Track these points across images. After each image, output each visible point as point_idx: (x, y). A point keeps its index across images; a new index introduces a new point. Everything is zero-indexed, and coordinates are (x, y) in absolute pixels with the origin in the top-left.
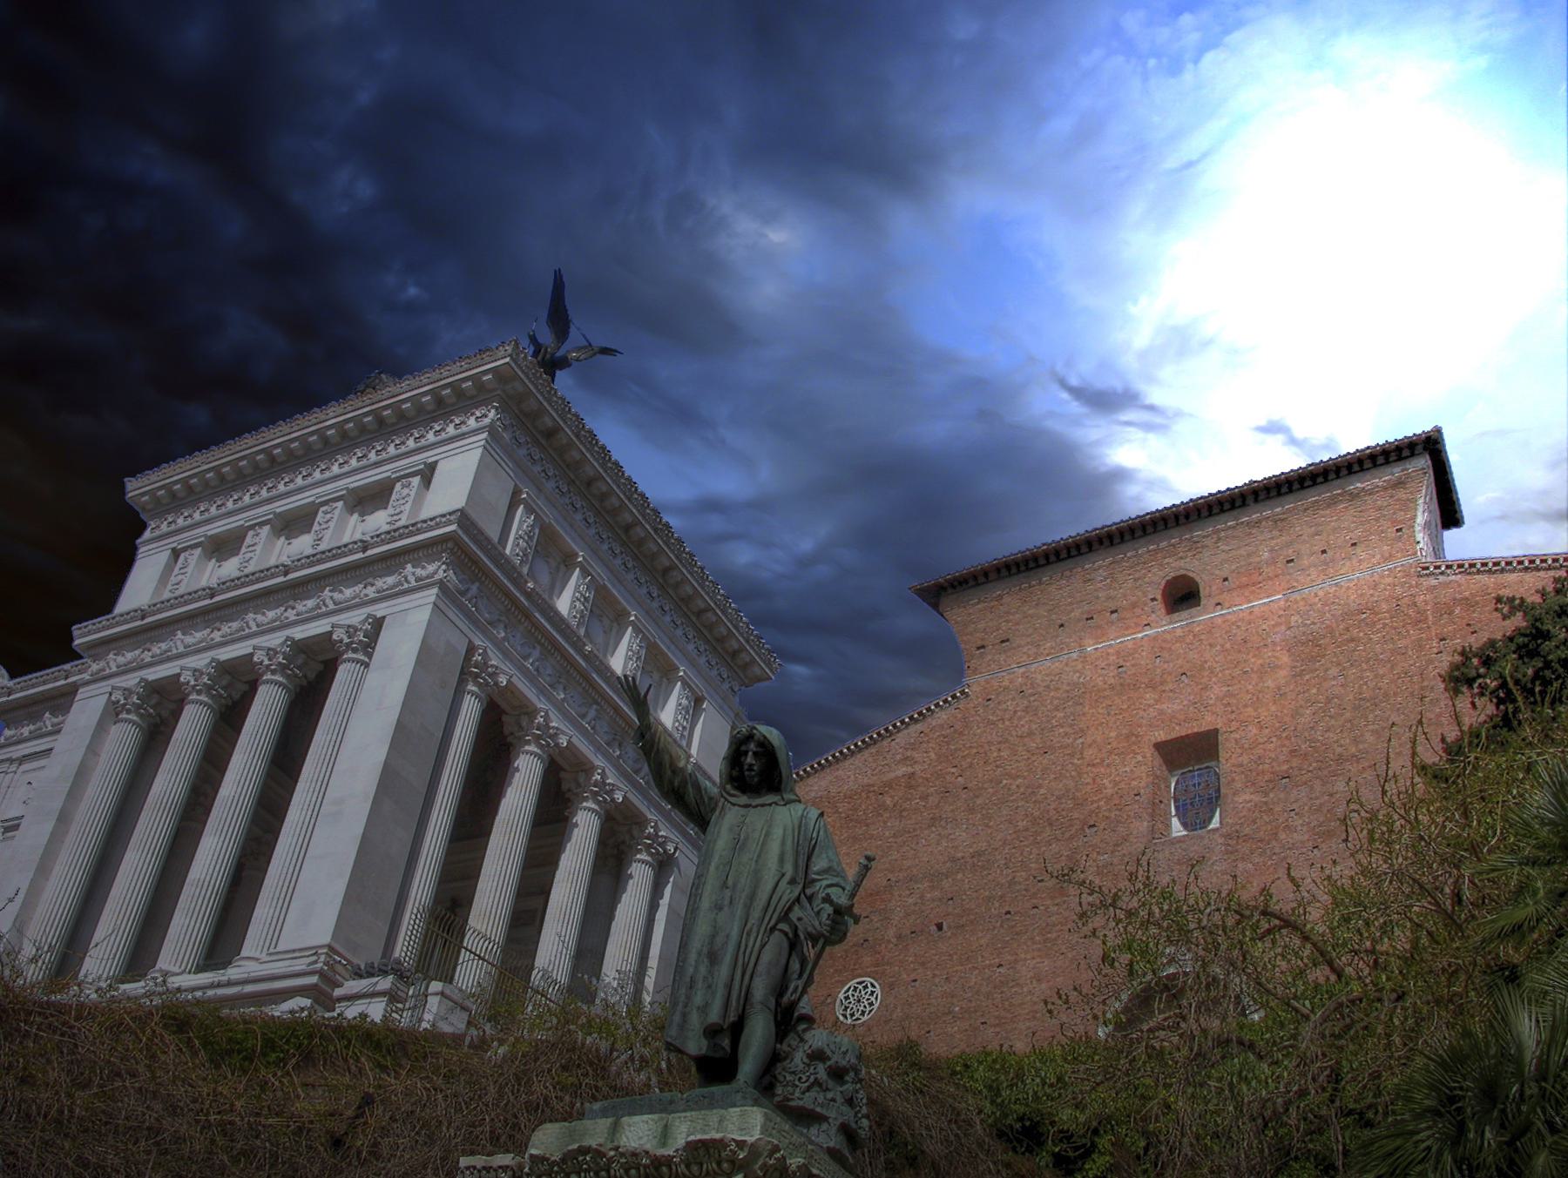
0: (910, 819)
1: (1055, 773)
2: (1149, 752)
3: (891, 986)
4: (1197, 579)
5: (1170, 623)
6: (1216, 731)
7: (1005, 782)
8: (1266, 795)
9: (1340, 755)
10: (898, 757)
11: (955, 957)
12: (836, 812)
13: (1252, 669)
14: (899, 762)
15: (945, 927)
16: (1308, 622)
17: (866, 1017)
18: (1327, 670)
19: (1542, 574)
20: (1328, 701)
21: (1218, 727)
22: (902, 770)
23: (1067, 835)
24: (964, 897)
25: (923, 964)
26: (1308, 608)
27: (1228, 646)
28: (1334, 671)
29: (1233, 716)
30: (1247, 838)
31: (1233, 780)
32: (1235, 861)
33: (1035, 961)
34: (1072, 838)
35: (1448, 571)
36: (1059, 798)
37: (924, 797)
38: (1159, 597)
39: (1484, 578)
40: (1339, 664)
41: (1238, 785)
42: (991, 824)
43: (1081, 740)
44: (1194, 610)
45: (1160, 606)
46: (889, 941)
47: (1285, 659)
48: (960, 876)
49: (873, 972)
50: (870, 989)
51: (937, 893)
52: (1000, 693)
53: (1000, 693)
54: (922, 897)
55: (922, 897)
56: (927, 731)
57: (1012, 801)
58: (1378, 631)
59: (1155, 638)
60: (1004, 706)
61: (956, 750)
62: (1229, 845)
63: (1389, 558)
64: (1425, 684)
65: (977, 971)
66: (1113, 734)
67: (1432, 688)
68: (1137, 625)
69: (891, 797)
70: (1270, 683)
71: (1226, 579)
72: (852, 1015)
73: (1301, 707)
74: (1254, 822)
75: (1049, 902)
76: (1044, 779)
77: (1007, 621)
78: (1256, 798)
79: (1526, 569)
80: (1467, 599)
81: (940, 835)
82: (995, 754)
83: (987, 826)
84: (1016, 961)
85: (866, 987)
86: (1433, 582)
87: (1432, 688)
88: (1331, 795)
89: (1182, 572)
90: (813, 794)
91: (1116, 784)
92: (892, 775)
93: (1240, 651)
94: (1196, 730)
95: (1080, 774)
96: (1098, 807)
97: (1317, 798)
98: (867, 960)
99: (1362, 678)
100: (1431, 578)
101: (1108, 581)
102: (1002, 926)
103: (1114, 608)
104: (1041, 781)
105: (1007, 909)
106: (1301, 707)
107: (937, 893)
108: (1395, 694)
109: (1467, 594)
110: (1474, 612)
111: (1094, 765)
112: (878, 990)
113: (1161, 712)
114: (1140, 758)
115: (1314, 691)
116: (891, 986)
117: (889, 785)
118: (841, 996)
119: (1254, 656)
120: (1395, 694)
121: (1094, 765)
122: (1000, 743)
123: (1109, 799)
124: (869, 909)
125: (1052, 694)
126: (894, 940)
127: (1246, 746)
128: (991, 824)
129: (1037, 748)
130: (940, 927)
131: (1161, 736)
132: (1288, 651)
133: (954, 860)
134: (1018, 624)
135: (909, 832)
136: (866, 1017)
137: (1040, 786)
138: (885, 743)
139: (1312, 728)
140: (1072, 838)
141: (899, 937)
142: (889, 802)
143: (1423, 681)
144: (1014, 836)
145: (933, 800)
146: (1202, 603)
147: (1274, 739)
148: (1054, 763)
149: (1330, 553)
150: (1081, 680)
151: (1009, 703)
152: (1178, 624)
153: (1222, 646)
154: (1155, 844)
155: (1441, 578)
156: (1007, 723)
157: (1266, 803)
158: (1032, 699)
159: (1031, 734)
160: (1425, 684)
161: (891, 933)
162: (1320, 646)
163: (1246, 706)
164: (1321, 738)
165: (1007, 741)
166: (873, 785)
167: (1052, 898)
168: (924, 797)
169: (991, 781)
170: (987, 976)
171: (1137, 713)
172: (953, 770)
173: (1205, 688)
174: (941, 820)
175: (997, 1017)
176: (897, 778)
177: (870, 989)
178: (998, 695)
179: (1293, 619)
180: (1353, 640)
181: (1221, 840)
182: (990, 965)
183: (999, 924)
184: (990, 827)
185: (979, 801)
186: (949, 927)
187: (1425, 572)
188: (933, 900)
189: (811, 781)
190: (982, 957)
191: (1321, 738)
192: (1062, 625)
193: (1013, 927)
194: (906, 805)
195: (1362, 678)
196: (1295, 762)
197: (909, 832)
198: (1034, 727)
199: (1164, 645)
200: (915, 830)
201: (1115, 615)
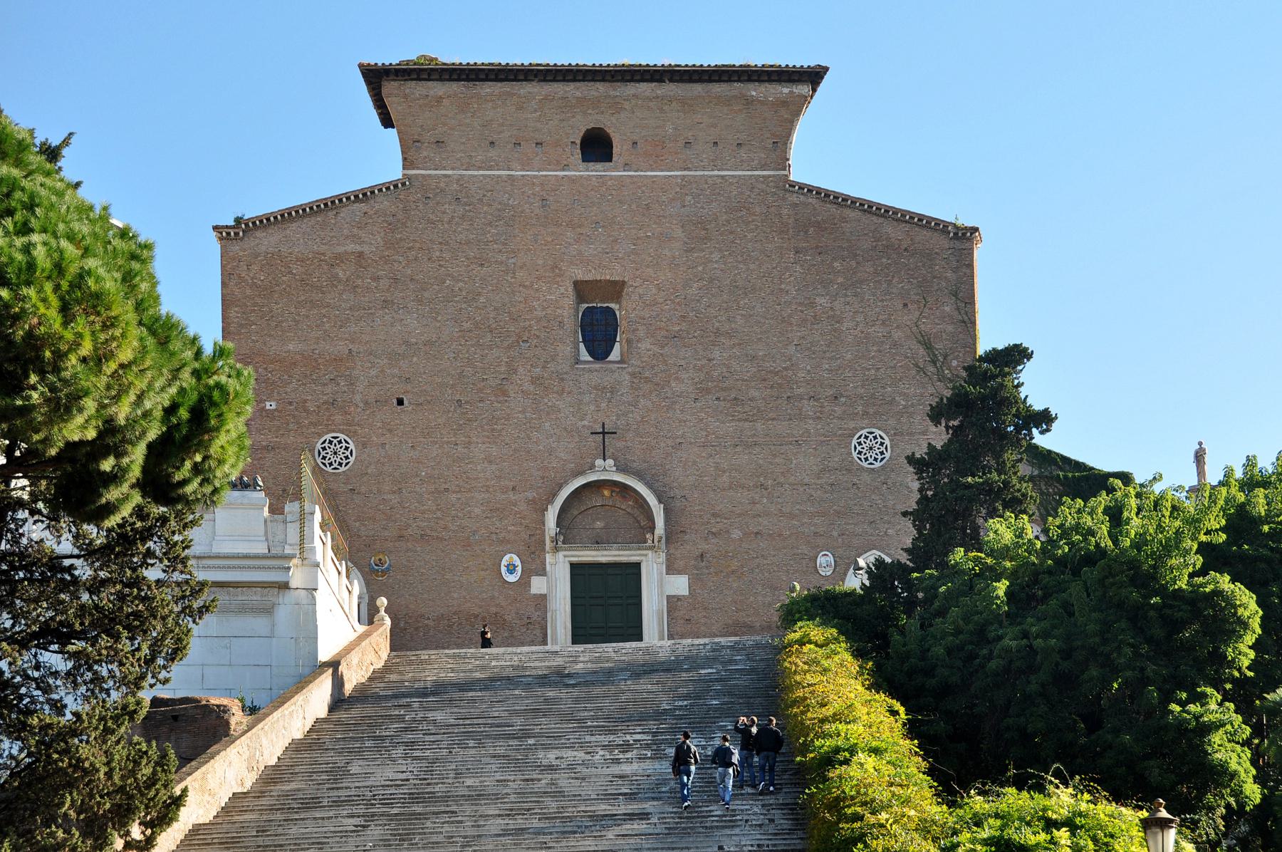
0: (364, 296)
1: (491, 285)
2: (571, 289)
3: (364, 445)
4: (612, 135)
5: (587, 170)
6: (624, 283)
7: (448, 281)
8: (663, 347)
9: (718, 329)
10: (346, 232)
11: (417, 430)
12: (290, 272)
13: (653, 234)
14: (347, 237)
15: (406, 402)
16: (699, 205)
17: (342, 469)
18: (711, 253)
19: (874, 218)
20: (711, 280)
21: (626, 280)
22: (351, 247)
23: (505, 344)
24: (420, 379)
25: (390, 431)
26: (699, 192)
27: (634, 207)
28: (716, 256)
29: (638, 273)
30: (647, 380)
31: (638, 330)
32: (638, 396)
33: (484, 446)
34: (509, 347)
35: (809, 194)
36: (496, 309)
37: (376, 279)
38: (578, 142)
39: (833, 209)
40: (720, 250)
41: (641, 333)
42: (439, 318)
43: (513, 260)
44: (607, 164)
45: (578, 152)
46: (357, 406)
47: (679, 233)
48: (415, 359)
49: (346, 430)
50: (344, 444)
51: (396, 371)
52: (437, 194)
53: (437, 194)
54: (382, 371)
55: (382, 371)
56: (372, 212)
57: (456, 302)
58: (752, 231)
59: (572, 180)
60: (443, 208)
61: (401, 239)
62: (633, 382)
63: (763, 167)
64: (783, 286)
65: (437, 446)
66: (540, 262)
67: (787, 292)
68: (558, 162)
69: (343, 270)
70: (666, 252)
71: (635, 143)
72: (331, 464)
73: (691, 280)
74: (653, 367)
75: (493, 398)
76: (483, 288)
77: (444, 124)
78: (656, 349)
79: (865, 211)
80: (819, 223)
81: (393, 318)
82: (438, 254)
83: (435, 319)
84: (470, 443)
85: (340, 442)
86: (794, 198)
87: (787, 292)
88: (710, 360)
89: (602, 126)
90: (264, 248)
91: (544, 309)
92: (341, 249)
93: (644, 215)
94: (608, 278)
95: (513, 292)
96: (530, 326)
97: (699, 360)
98: (338, 418)
99: (737, 268)
100: (795, 195)
101: (538, 114)
102: (455, 411)
103: (539, 141)
104: (480, 290)
105: (458, 397)
106: (691, 280)
107: (396, 371)
108: (761, 289)
109: (819, 218)
110: (823, 236)
111: (525, 286)
112: (352, 446)
113: (580, 253)
114: (562, 291)
115: (700, 268)
116: (364, 445)
117: (340, 258)
118: (319, 446)
119: (655, 223)
120: (761, 289)
121: (525, 286)
122: (441, 243)
123: (539, 320)
124: (335, 373)
125: (485, 208)
126: (361, 405)
127: (648, 302)
128: (439, 318)
129: (475, 258)
130: (400, 402)
131: (580, 277)
132: (682, 227)
133: (407, 343)
134: (452, 129)
135: (365, 309)
136: (342, 469)
137: (479, 294)
138: (331, 214)
139: (698, 301)
140: (509, 347)
141: (366, 403)
142: (341, 274)
143: (781, 283)
144: (460, 334)
145: (384, 283)
146: (614, 159)
147: (669, 302)
148: (490, 276)
149: (720, 147)
150: (510, 202)
151: (447, 206)
152: (596, 171)
153: (630, 205)
154: (577, 368)
155: (802, 197)
156: (446, 225)
157: (661, 355)
158: (467, 208)
159: (468, 243)
160: (783, 286)
161: (358, 397)
162: (707, 229)
163: (648, 266)
164: (703, 311)
165: (447, 243)
166: (323, 254)
167: (496, 395)
168: (376, 279)
169: (436, 278)
170: (446, 450)
171: (560, 249)
172: (401, 259)
173: (616, 241)
174: (394, 304)
175: (458, 486)
176: (346, 252)
177: (344, 444)
178: (436, 195)
179: (689, 198)
180: (731, 233)
181: (627, 377)
182: (448, 442)
183: (452, 409)
184: (437, 321)
185: (426, 295)
186: (410, 403)
187: (791, 189)
188: (394, 377)
189: (259, 234)
190: (441, 434)
191: (703, 311)
192: (492, 143)
193: (465, 413)
194: (359, 282)
195: (737, 268)
196: (684, 326)
197: (365, 309)
198: (472, 236)
199: (581, 189)
200: (370, 309)
201: (539, 150)
